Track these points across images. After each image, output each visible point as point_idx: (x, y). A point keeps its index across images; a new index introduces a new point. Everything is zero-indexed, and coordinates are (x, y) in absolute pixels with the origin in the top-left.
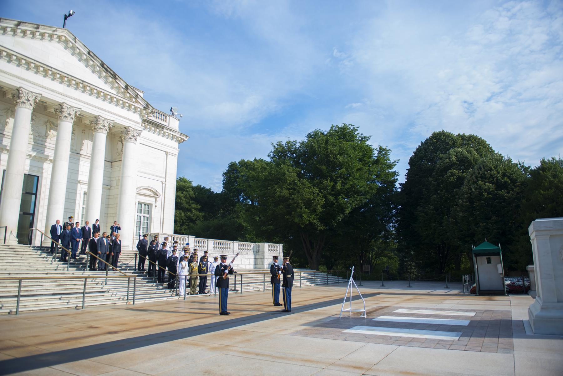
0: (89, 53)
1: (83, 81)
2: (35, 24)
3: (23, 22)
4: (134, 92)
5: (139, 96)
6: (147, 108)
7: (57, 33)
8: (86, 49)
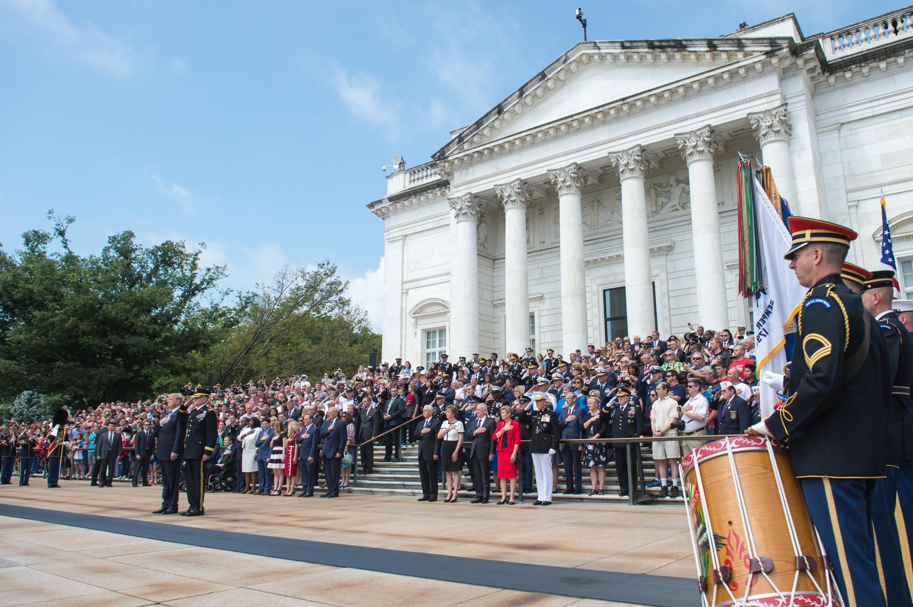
0: (623, 47)
1: (623, 99)
2: (538, 75)
3: (524, 86)
4: (731, 42)
5: (743, 41)
6: (777, 48)
7: (572, 60)
8: (617, 44)
